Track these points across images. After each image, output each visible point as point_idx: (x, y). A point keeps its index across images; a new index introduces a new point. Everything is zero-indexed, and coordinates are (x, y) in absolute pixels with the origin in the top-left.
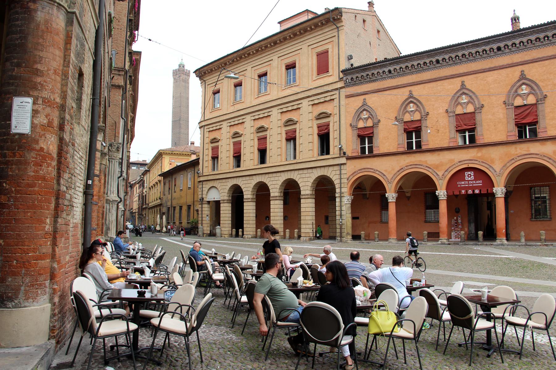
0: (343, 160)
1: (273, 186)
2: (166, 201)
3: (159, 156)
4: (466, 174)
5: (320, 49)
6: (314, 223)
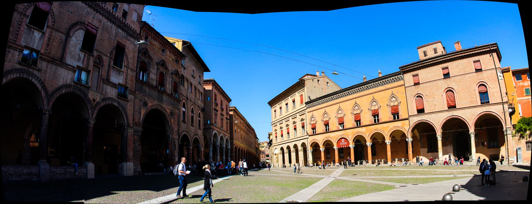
0: (308, 137)
4: (343, 140)
6: (303, 160)
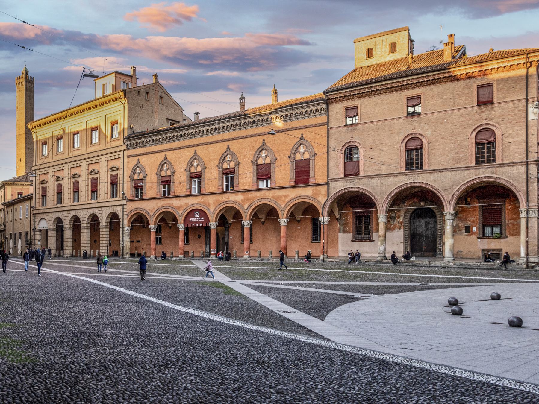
0: (124, 202)
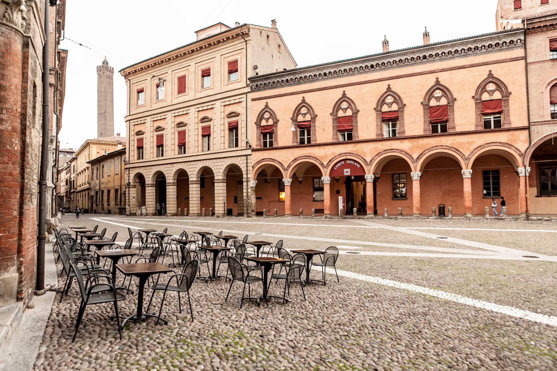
0: (249, 152)
1: (191, 173)
2: (94, 185)
3: (87, 145)
5: (231, 59)
6: (226, 202)
